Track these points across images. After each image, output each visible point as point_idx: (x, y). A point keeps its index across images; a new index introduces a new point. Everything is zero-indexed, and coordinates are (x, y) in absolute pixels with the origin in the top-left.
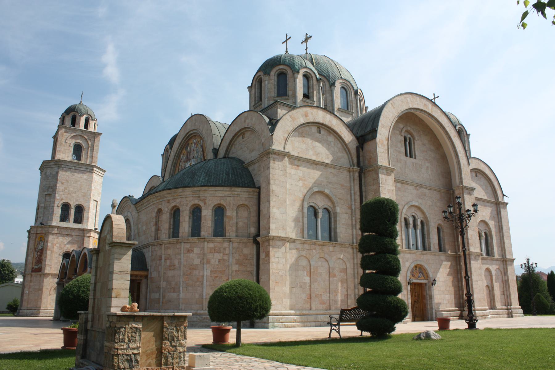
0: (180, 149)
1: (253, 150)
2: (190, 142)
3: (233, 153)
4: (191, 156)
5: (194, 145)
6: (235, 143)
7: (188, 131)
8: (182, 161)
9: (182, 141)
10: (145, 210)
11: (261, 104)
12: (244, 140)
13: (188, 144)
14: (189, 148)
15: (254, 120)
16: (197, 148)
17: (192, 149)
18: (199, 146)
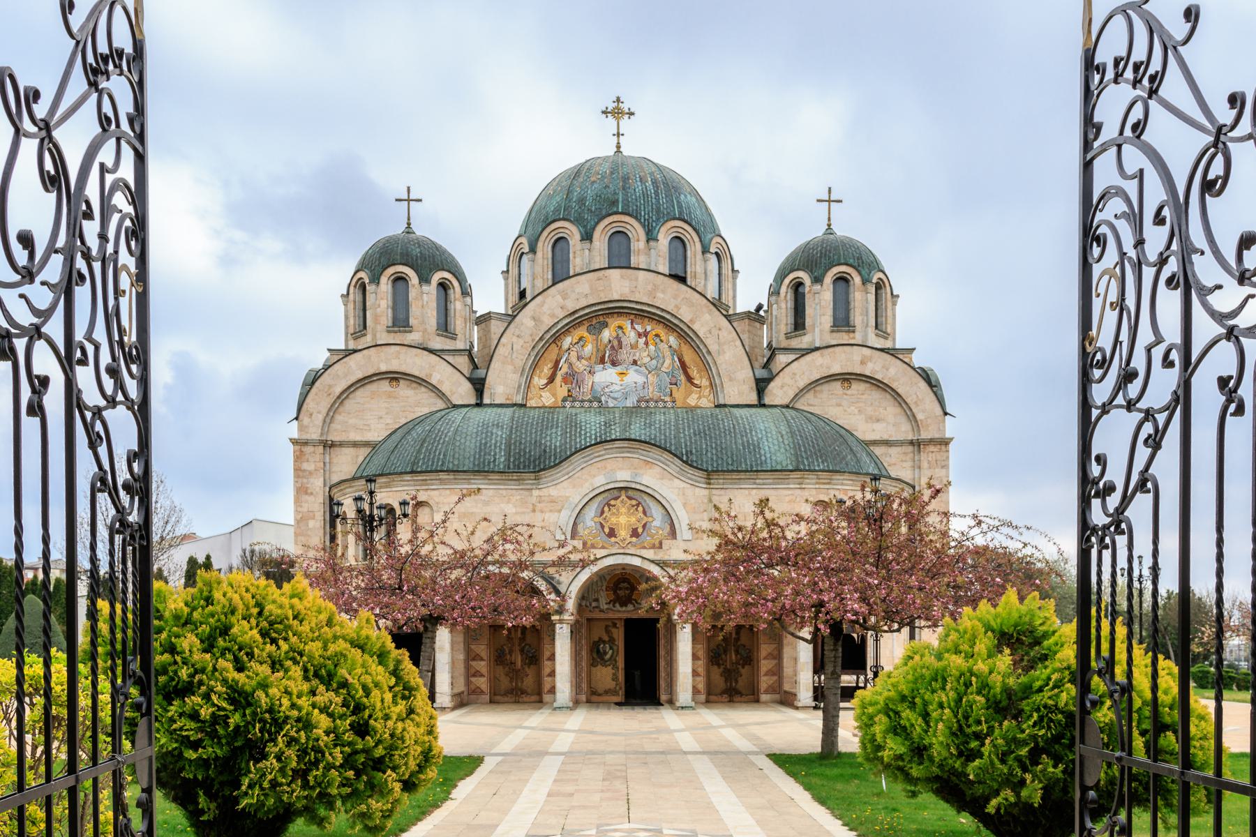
0: (567, 325)
1: (878, 421)
2: (614, 322)
3: (809, 405)
4: (624, 355)
5: (633, 335)
6: (818, 388)
7: (616, 297)
8: (573, 355)
9: (583, 308)
10: (754, 491)
11: (854, 332)
12: (849, 392)
13: (606, 325)
14: (606, 334)
15: (892, 371)
16: (652, 348)
17: (625, 341)
18: (663, 346)
